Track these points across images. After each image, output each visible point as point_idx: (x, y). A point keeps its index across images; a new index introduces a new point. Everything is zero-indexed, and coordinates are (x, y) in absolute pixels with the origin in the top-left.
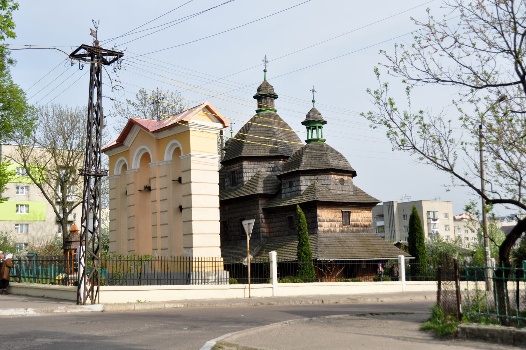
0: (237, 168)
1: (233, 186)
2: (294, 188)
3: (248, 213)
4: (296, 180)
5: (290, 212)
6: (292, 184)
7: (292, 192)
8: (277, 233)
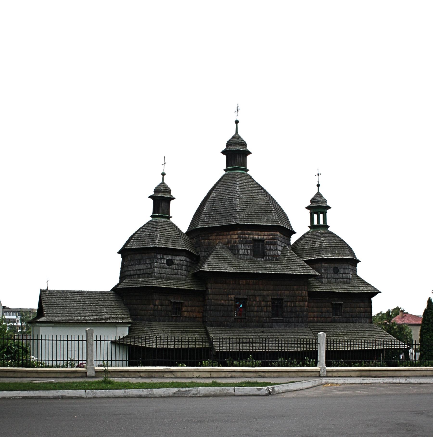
0: (265, 237)
1: (257, 258)
2: (341, 275)
3: (287, 293)
4: (343, 267)
5: (336, 299)
6: (338, 271)
7: (338, 278)
8: (315, 319)
